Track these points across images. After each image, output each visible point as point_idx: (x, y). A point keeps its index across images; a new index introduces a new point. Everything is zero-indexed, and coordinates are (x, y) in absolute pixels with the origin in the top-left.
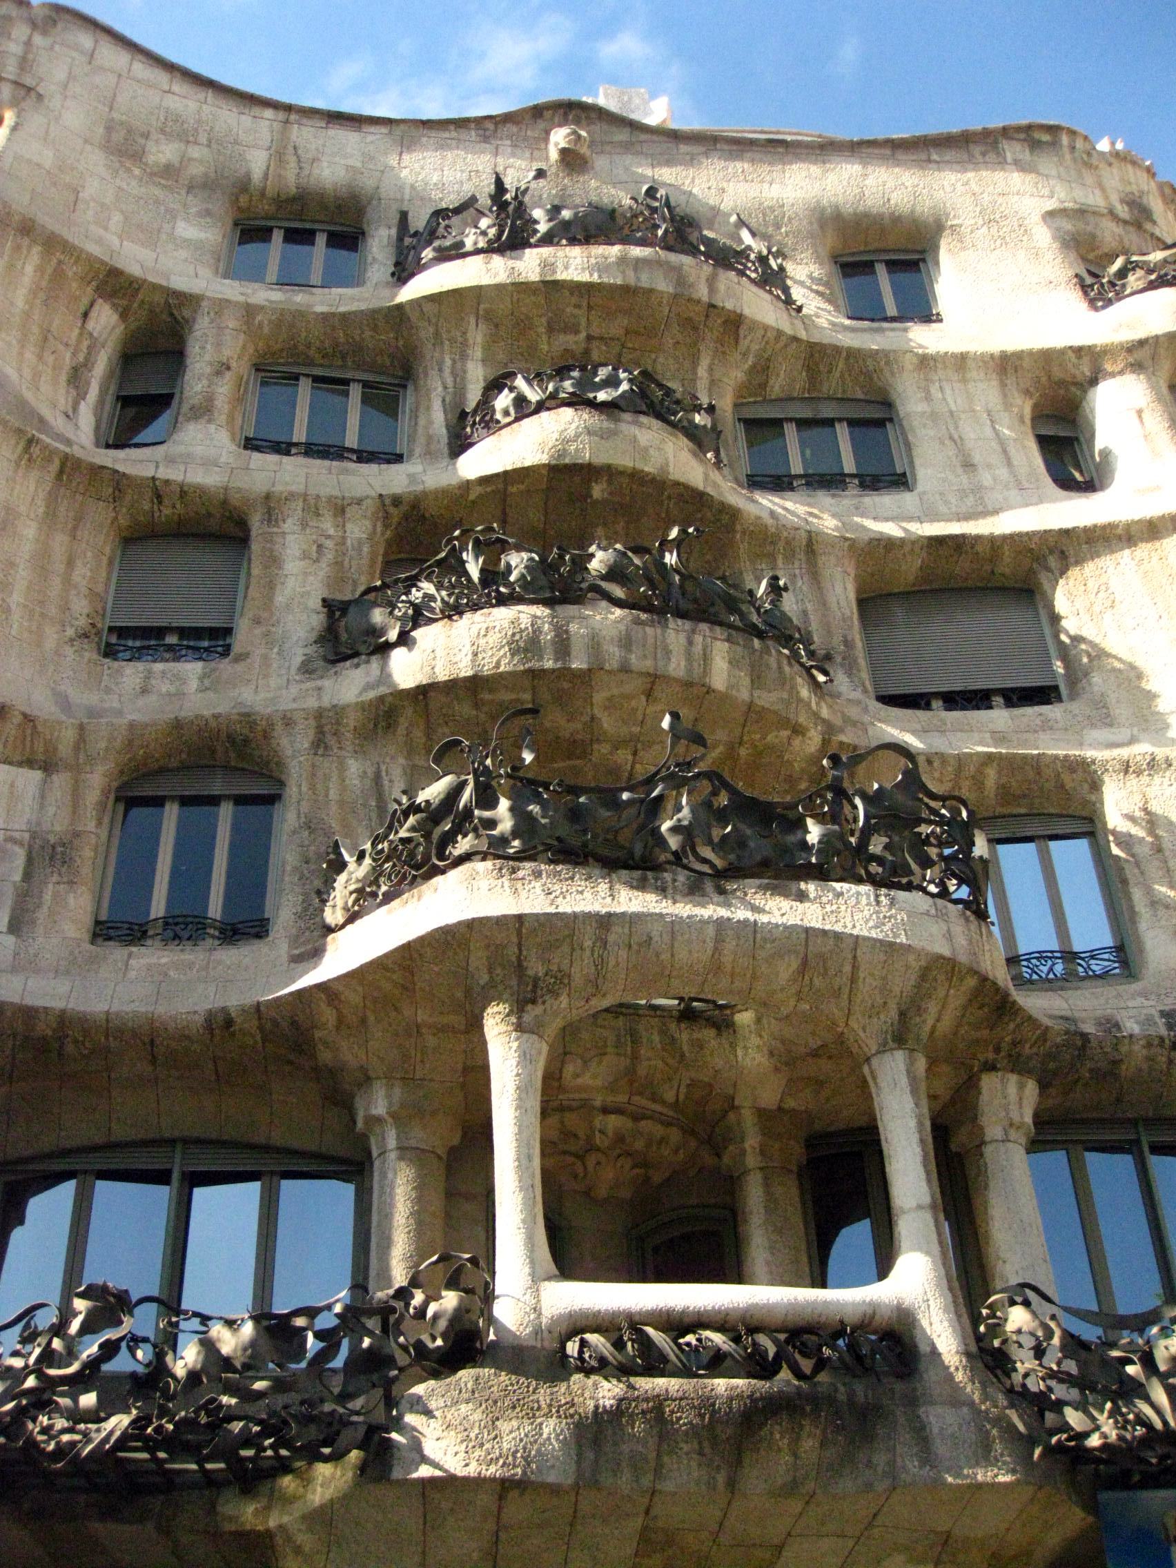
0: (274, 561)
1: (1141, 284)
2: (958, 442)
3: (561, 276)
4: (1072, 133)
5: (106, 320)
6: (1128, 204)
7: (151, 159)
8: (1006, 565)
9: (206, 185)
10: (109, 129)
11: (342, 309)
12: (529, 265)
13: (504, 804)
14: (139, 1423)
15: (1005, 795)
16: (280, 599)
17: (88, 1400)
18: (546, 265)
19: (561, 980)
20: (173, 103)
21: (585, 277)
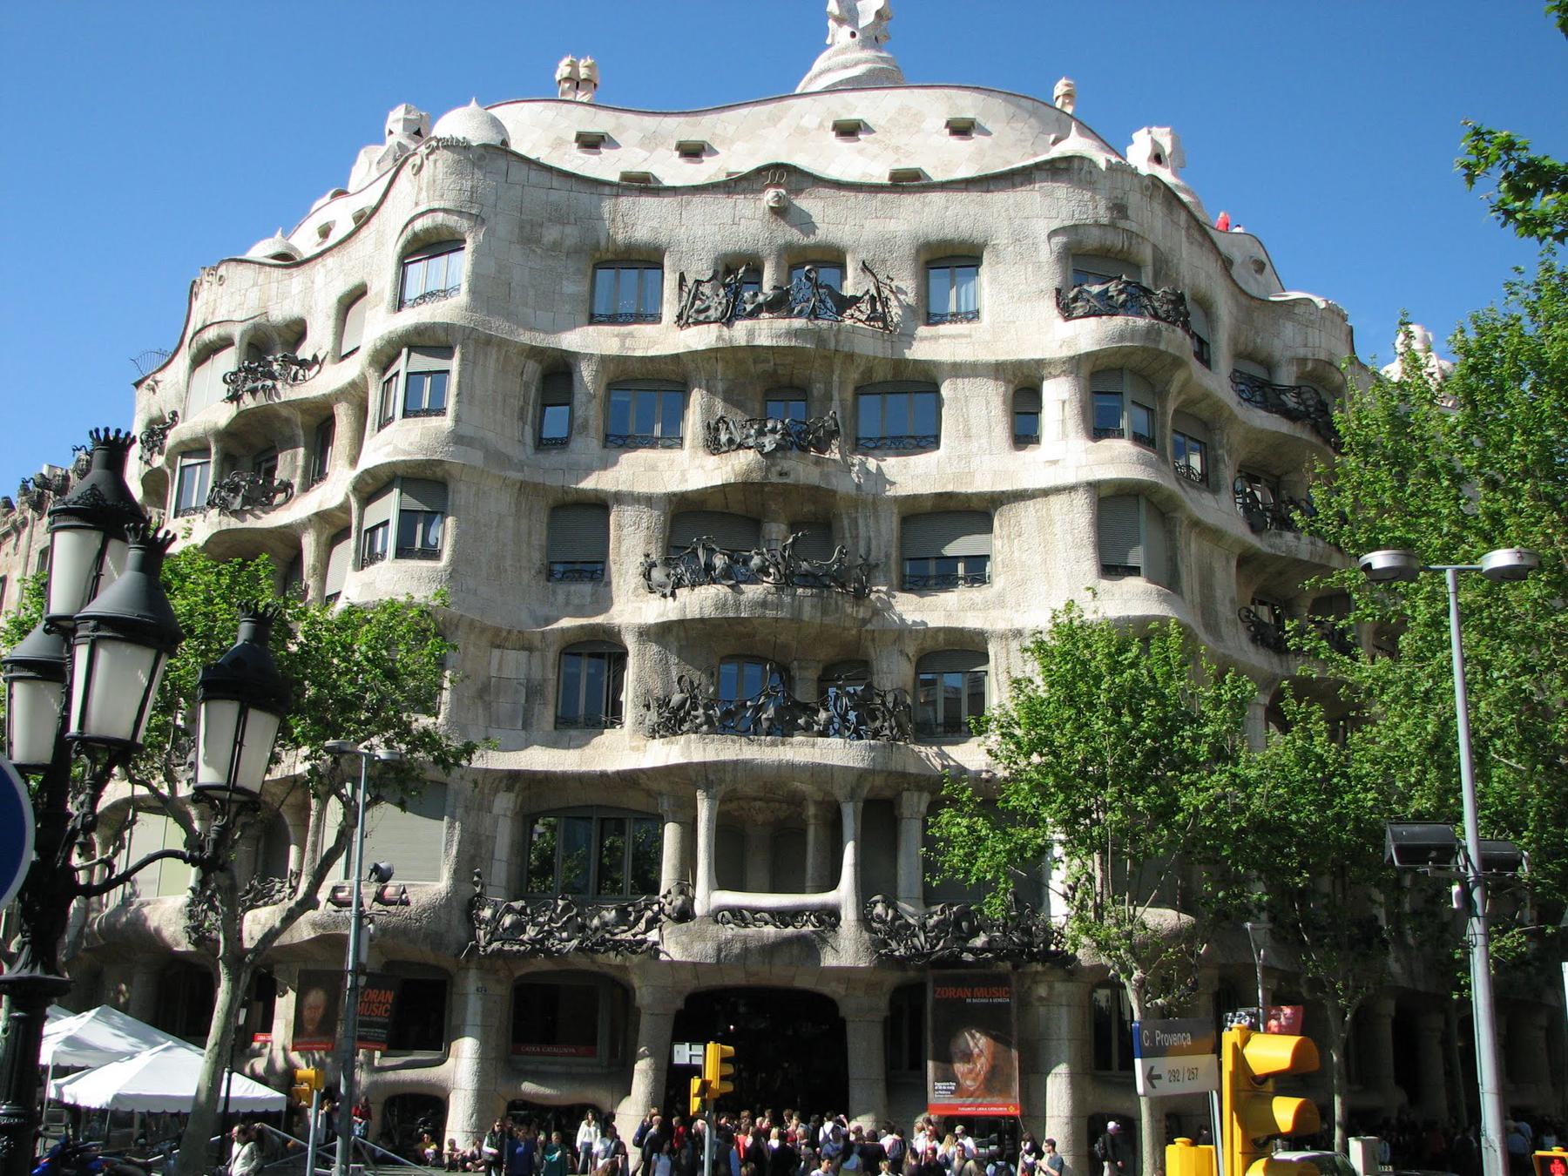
0: (620, 527)
1: (1079, 312)
2: (966, 421)
3: (757, 343)
4: (1082, 158)
5: (533, 368)
6: (1108, 208)
7: (545, 240)
8: (975, 504)
9: (576, 251)
10: (522, 228)
11: (651, 353)
12: (740, 332)
13: (701, 711)
14: (581, 943)
15: (947, 642)
16: (623, 549)
17: (565, 935)
18: (751, 333)
19: (721, 781)
20: (555, 196)
21: (767, 343)
